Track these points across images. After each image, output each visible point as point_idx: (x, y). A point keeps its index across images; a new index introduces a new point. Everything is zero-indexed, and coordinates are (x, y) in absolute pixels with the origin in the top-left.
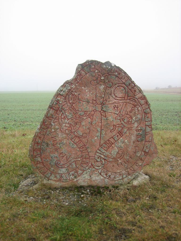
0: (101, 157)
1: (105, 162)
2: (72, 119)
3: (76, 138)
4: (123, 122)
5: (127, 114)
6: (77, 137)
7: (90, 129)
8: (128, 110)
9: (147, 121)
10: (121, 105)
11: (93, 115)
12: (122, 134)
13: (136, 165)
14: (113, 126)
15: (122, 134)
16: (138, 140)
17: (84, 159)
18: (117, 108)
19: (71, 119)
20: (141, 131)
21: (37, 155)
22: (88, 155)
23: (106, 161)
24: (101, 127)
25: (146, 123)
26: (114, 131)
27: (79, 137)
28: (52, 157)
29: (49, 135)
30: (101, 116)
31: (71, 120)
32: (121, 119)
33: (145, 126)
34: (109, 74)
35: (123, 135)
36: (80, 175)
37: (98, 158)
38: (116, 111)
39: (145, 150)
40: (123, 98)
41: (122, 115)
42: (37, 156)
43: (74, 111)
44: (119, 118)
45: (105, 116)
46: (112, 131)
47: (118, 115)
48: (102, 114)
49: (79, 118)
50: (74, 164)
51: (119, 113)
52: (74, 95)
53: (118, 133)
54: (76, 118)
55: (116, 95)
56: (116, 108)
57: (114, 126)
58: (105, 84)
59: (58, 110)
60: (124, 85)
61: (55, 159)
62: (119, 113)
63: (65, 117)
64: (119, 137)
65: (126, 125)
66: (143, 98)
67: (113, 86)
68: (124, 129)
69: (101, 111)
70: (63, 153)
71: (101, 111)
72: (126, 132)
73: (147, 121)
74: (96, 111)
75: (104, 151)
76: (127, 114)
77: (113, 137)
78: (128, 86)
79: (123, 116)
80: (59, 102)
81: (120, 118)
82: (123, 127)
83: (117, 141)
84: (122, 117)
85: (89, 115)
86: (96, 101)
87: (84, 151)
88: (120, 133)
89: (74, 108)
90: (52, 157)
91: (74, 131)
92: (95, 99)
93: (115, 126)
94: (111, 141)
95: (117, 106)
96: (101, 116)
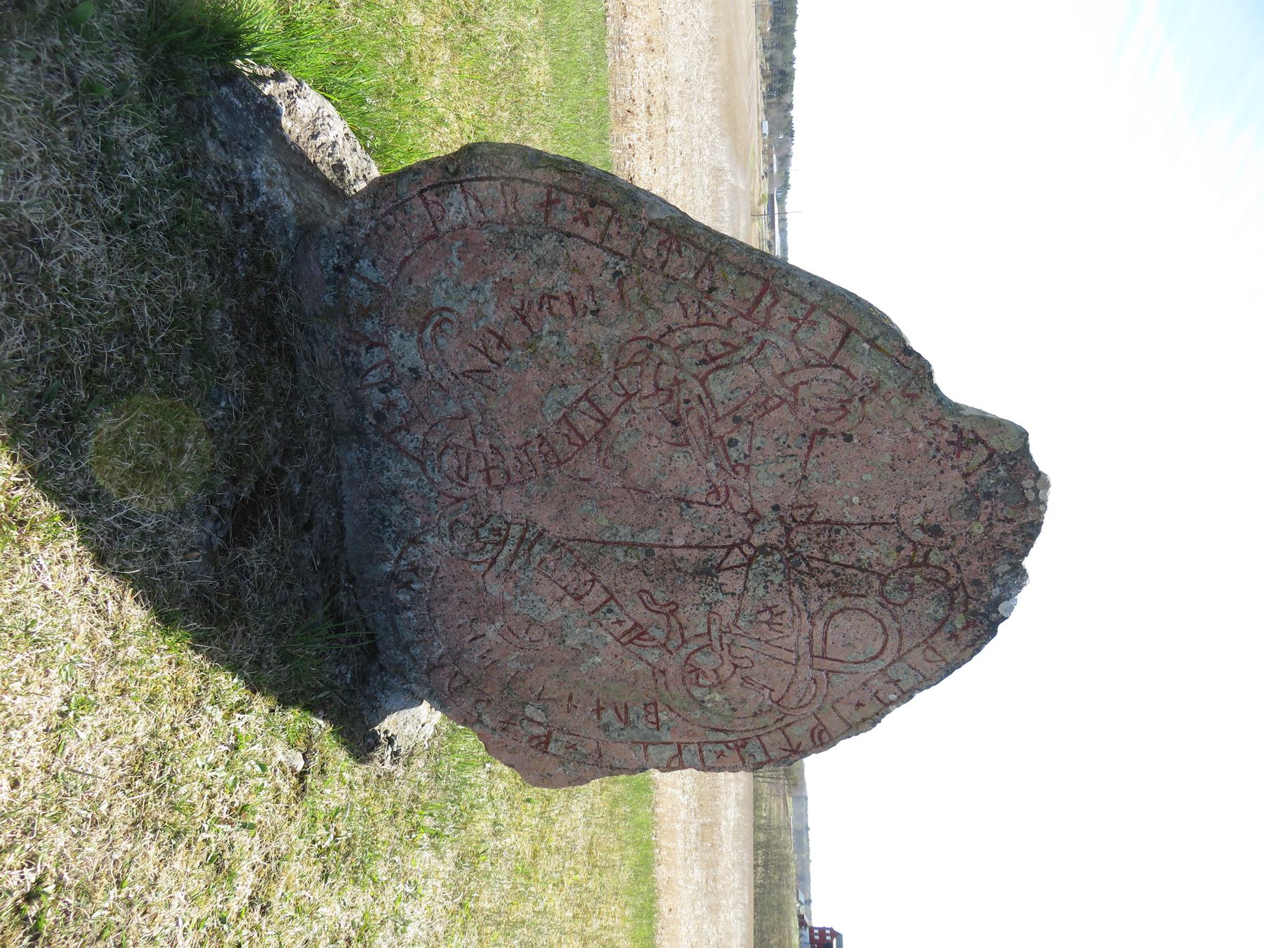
1: (478, 563)
4: (693, 646)
5: (736, 666)
6: (599, 426)
7: (649, 493)
8: (756, 669)
9: (701, 751)
12: (631, 641)
15: (631, 641)
16: (603, 709)
17: (486, 464)
19: (703, 396)
21: (476, 199)
23: (482, 568)
24: (665, 547)
25: (694, 748)
26: (646, 607)
28: (474, 289)
29: (607, 275)
30: (723, 547)
31: (699, 397)
32: (710, 640)
35: (623, 645)
40: (824, 651)
41: (729, 645)
42: (473, 203)
44: (713, 628)
46: (645, 597)
48: (736, 550)
51: (738, 632)
52: (841, 413)
53: (636, 625)
55: (839, 619)
57: (673, 607)
59: (754, 321)
60: (888, 656)
61: (464, 309)
63: (714, 359)
64: (619, 630)
66: (820, 738)
68: (657, 651)
69: (751, 545)
70: (507, 353)
71: (751, 545)
73: (701, 751)
76: (736, 666)
78: (885, 675)
79: (726, 650)
81: (715, 634)
84: (721, 646)
88: (634, 634)
90: (474, 289)
94: (590, 590)
96: (723, 547)
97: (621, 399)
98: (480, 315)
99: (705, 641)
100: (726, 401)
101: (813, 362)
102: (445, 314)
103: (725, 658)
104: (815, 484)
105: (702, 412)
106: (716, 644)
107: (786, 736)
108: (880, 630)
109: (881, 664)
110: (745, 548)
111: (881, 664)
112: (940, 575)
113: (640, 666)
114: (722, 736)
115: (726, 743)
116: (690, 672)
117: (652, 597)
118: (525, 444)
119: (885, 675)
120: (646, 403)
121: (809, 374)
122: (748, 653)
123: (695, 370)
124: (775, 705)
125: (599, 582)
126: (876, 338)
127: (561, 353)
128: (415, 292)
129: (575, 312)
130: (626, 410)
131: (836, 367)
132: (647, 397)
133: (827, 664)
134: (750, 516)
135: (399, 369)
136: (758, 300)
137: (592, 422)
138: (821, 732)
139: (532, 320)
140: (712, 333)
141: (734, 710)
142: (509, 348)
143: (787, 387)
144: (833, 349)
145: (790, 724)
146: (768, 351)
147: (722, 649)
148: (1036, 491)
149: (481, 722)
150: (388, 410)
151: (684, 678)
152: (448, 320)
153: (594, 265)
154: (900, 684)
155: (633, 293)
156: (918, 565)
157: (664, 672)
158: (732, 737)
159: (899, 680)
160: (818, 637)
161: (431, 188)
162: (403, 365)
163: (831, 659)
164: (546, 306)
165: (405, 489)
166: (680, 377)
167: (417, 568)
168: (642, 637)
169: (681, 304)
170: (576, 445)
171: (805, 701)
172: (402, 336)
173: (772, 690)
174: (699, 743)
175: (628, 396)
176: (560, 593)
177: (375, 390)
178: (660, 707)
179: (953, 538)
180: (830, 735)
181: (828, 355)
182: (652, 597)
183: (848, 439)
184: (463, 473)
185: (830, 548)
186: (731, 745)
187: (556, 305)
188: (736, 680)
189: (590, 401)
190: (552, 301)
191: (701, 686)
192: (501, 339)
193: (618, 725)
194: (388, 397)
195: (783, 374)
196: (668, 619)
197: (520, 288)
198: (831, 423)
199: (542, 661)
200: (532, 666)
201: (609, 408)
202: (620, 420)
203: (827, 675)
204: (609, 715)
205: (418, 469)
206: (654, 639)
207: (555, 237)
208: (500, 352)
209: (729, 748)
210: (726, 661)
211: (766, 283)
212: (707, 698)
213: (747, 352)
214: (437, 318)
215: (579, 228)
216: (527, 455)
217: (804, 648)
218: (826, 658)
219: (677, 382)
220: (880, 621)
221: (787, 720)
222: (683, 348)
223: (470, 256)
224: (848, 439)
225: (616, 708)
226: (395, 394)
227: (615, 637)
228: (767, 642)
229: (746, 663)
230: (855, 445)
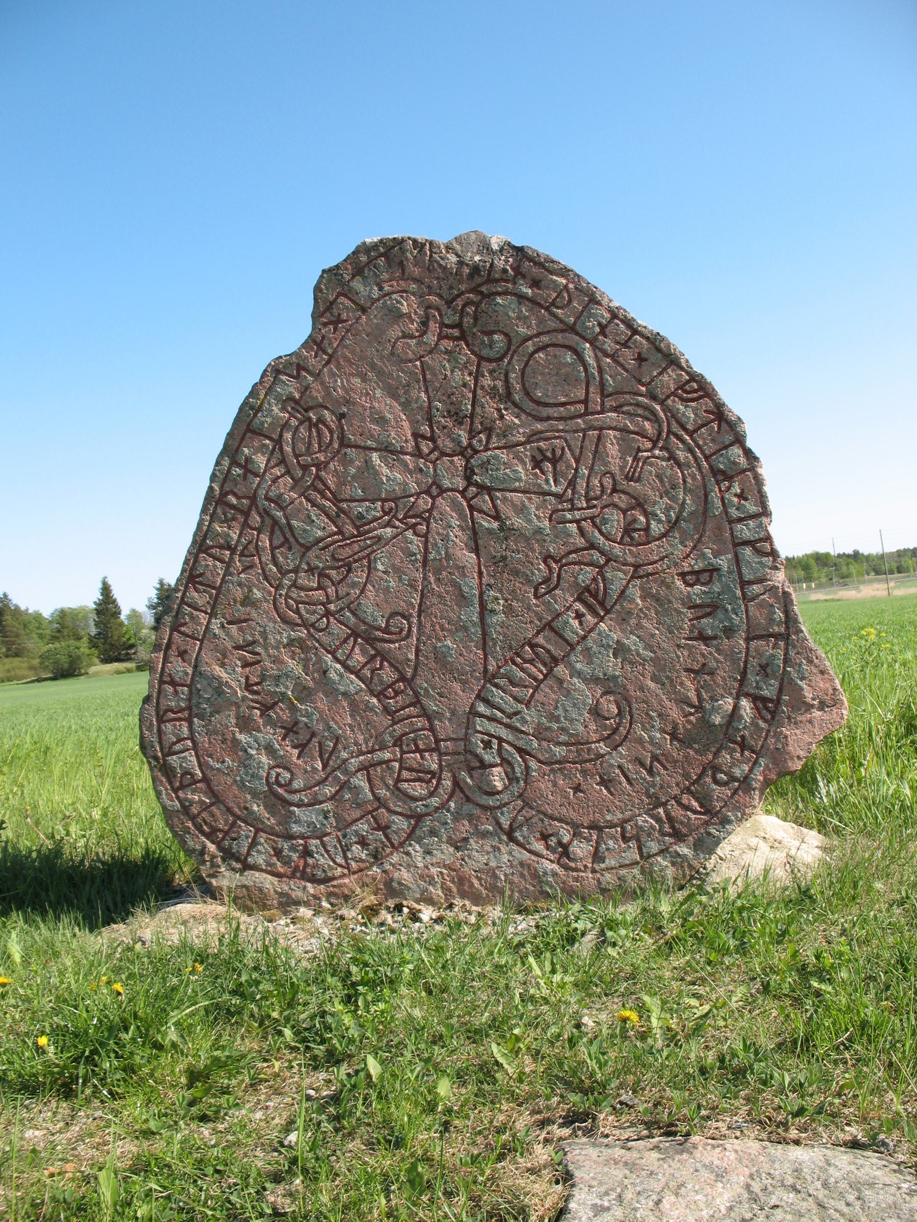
2: (323, 549)
3: (355, 642)
5: (614, 490)
10: (572, 443)
11: (426, 517)
14: (545, 562)
15: (602, 604)
16: (700, 633)
17: (413, 752)
18: (554, 461)
20: (711, 577)
22: (432, 729)
27: (370, 641)
33: (735, 545)
36: (402, 844)
38: (552, 482)
39: (758, 687)
40: (580, 402)
43: (327, 504)
45: (493, 513)
47: (565, 498)
49: (356, 536)
50: (360, 781)
51: (570, 491)
53: (579, 599)
56: (548, 466)
58: (467, 345)
62: (565, 491)
63: (287, 540)
64: (590, 619)
65: (617, 549)
66: (695, 391)
67: (513, 348)
71: (465, 489)
72: (623, 592)
74: (442, 491)
75: (510, 704)
76: (614, 490)
77: (554, 624)
81: (577, 515)
82: (602, 561)
83: (578, 642)
84: (588, 508)
85: (405, 517)
86: (432, 439)
87: (403, 708)
89: (329, 489)
91: (342, 609)
92: (425, 429)
93: (556, 562)
95: (549, 454)
99: (586, 525)
116: (632, 538)
117: (541, 584)
134: (434, 491)
147: (595, 506)
157: (637, 567)
182: (541, 584)
185: (456, 414)
193: (720, 614)
208: (301, 731)
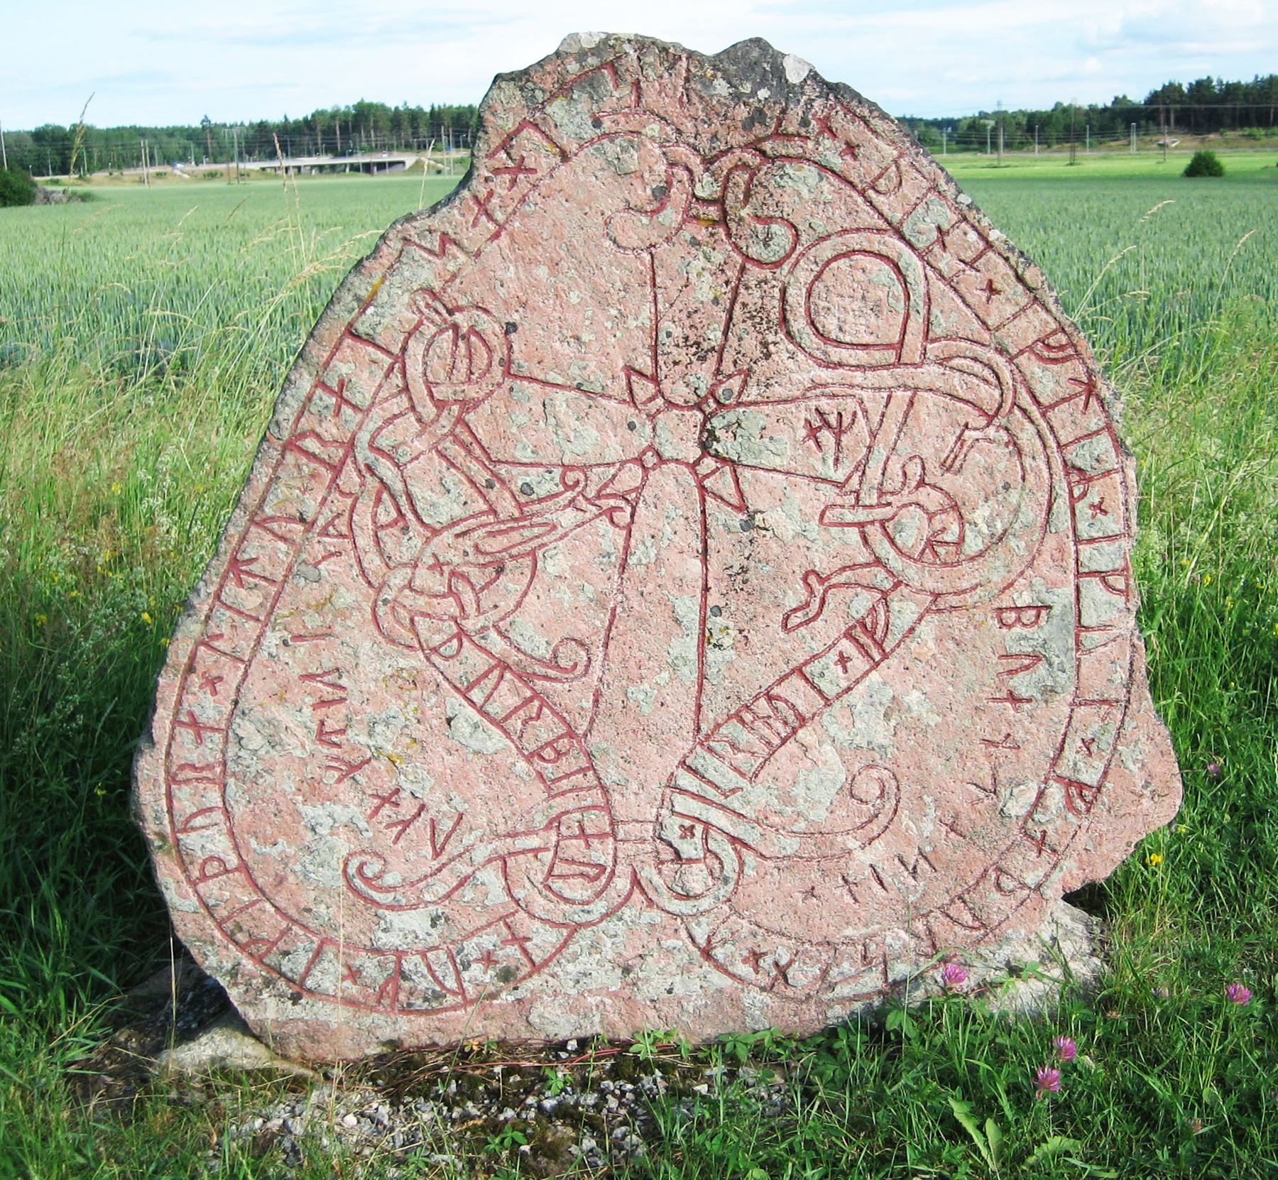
0: (707, 825)
1: (742, 864)
2: (464, 534)
3: (501, 677)
4: (884, 550)
5: (922, 483)
6: (508, 675)
7: (614, 610)
8: (927, 452)
9: (1092, 540)
10: (868, 405)
11: (632, 499)
12: (880, 645)
13: (998, 887)
14: (805, 579)
15: (880, 645)
17: (576, 837)
18: (839, 432)
19: (458, 530)
20: (1038, 616)
21: (194, 816)
22: (608, 807)
23: (749, 857)
24: (706, 589)
25: (1086, 550)
26: (814, 619)
27: (525, 677)
28: (313, 829)
29: (285, 655)
30: (703, 501)
31: (457, 536)
32: (872, 522)
33: (1078, 575)
34: (763, 153)
35: (885, 656)
36: (546, 963)
37: (688, 832)
38: (831, 461)
39: (1075, 768)
40: (889, 346)
41: (881, 494)
42: (198, 821)
43: (475, 466)
44: (849, 517)
45: (735, 500)
46: (794, 621)
47: (848, 488)
48: (707, 483)
49: (516, 520)
50: (491, 877)
51: (856, 479)
52: (473, 338)
53: (848, 635)
54: (491, 518)
55: (830, 324)
56: (827, 437)
57: (812, 580)
58: (729, 235)
59: (343, 463)
60: (893, 246)
61: (343, 845)
62: (850, 477)
64: (859, 663)
65: (912, 572)
66: (1061, 348)
67: (800, 249)
68: (895, 606)
69: (697, 462)
70: (403, 795)
71: (697, 462)
72: (912, 630)
73: (1092, 540)
74: (662, 460)
75: (729, 779)
76: (922, 483)
77: (807, 670)
78: (929, 251)
79: (890, 498)
80: (346, 394)
81: (862, 515)
82: (888, 585)
83: (838, 696)
84: (880, 505)
85: (598, 496)
86: (655, 379)
87: (567, 776)
88: (864, 639)
89: (479, 443)
90: (313, 829)
91: (484, 628)
92: (645, 363)
93: (821, 580)
94: (786, 702)
95: (833, 420)
96: (703, 501)
97: (466, 643)
98: (351, 825)
99: (874, 532)
100: (463, 499)
101: (400, 382)
102: (352, 870)
103: (905, 500)
104: (588, 371)
105: (481, 532)
106: (880, 513)
107: (1057, 404)
108: (843, 263)
109: (909, 259)
110: (703, 469)
111: (909, 259)
112: (741, 178)
113: (927, 630)
114: (1062, 505)
115: (1073, 500)
116: (936, 554)
117: (795, 610)
118: (544, 781)
119: (929, 251)
120: (471, 609)
121: (418, 389)
122: (895, 468)
123: (418, 542)
124: (996, 422)
125: (771, 687)
126: (358, 299)
127: (401, 721)
128: (323, 906)
129: (342, 700)
130: (483, 638)
131: (404, 349)
132: (463, 609)
133: (914, 340)
134: (650, 459)
135: (434, 940)
136: (313, 457)
137: (504, 686)
138: (1048, 347)
139: (355, 758)
140: (363, 518)
141: (1007, 487)
142: (397, 791)
143: (438, 416)
144: (380, 355)
145: (1034, 397)
146: (384, 442)
147: (889, 504)
148: (582, 56)
149: (1039, 886)
150: (497, 962)
151: (945, 564)
152: (360, 869)
153: (274, 672)
154: (945, 227)
155: (313, 621)
156: (725, 213)
157: (937, 596)
158: (1062, 488)
159: (939, 228)
160: (862, 356)
161: (185, 870)
162: (429, 935)
163: (904, 333)
164: (334, 739)
165: (620, 955)
166: (431, 561)
167: (754, 954)
168: (869, 626)
169: (324, 558)
170: (540, 709)
171: (987, 373)
172: (385, 930)
173: (966, 426)
174: (799, 671)
175: (461, 634)
176: (791, 746)
177: (466, 975)
178: (1006, 602)
179: (672, 164)
180: (1054, 332)
181: (388, 361)
182: (795, 610)
183: (511, 328)
184: (592, 872)
185: (698, 344)
186: (1077, 493)
187: (331, 725)
188: (948, 481)
189: (471, 687)
190: (327, 729)
191: (962, 539)
192: (385, 800)
193: (1042, 669)
194: (477, 960)
195: (419, 420)
196: (834, 586)
197: (313, 770)
198: (490, 350)
199: (918, 781)
200: (927, 799)
201: (479, 662)
202: (497, 644)
203: (933, 341)
204: (1023, 684)
205: (587, 932)
206: (874, 608)
207: (238, 720)
208: (403, 803)
209: (1084, 494)
210: (913, 498)
211: (289, 446)
212: (985, 530)
213: (386, 469)
214: (358, 882)
215: (227, 689)
216: (559, 779)
217: (885, 377)
218: (902, 342)
219: (438, 566)
220: (828, 263)
221: (1025, 400)
222: (387, 559)
223: (269, 831)
224: (511, 328)
225: (1010, 672)
226: (471, 948)
227: (872, 669)
228: (873, 435)
229: (915, 470)
230: (523, 318)
